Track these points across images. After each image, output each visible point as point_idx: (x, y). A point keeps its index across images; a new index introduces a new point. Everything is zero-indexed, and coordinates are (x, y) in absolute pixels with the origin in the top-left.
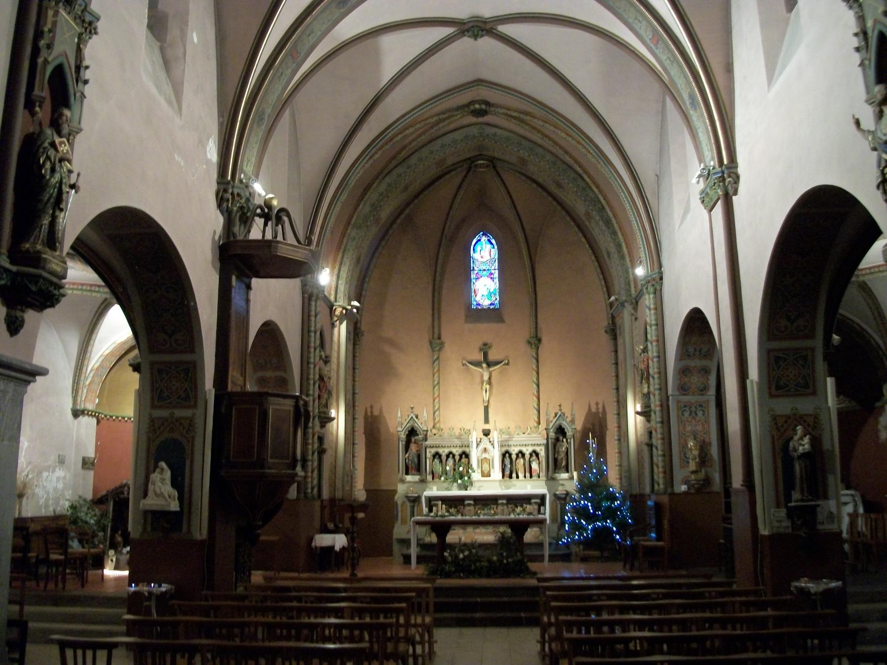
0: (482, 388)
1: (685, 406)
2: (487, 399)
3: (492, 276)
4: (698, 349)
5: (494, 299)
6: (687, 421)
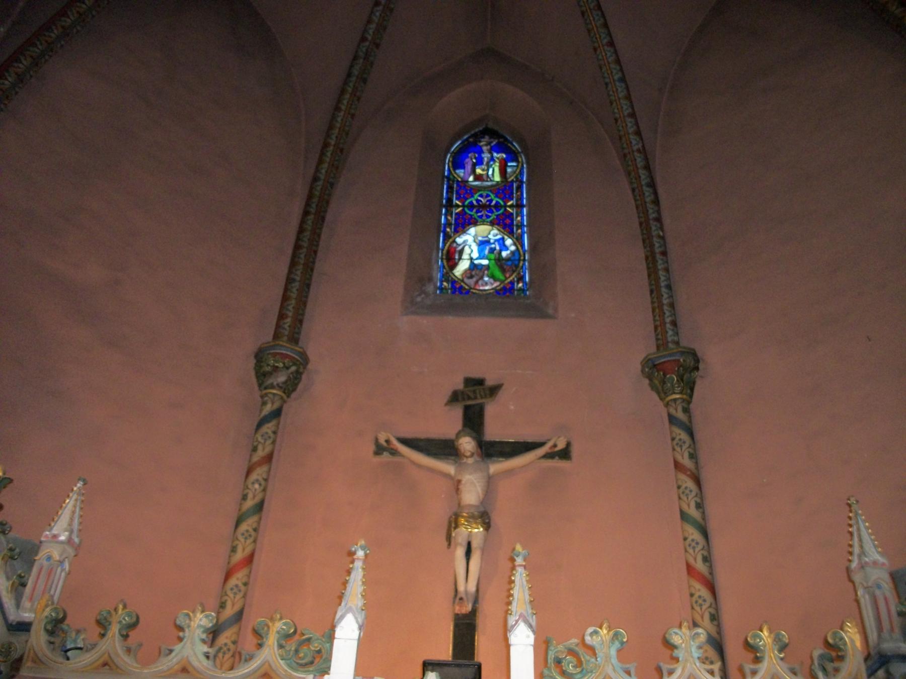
0: (449, 538)
2: (472, 587)
3: (508, 221)
5: (514, 277)
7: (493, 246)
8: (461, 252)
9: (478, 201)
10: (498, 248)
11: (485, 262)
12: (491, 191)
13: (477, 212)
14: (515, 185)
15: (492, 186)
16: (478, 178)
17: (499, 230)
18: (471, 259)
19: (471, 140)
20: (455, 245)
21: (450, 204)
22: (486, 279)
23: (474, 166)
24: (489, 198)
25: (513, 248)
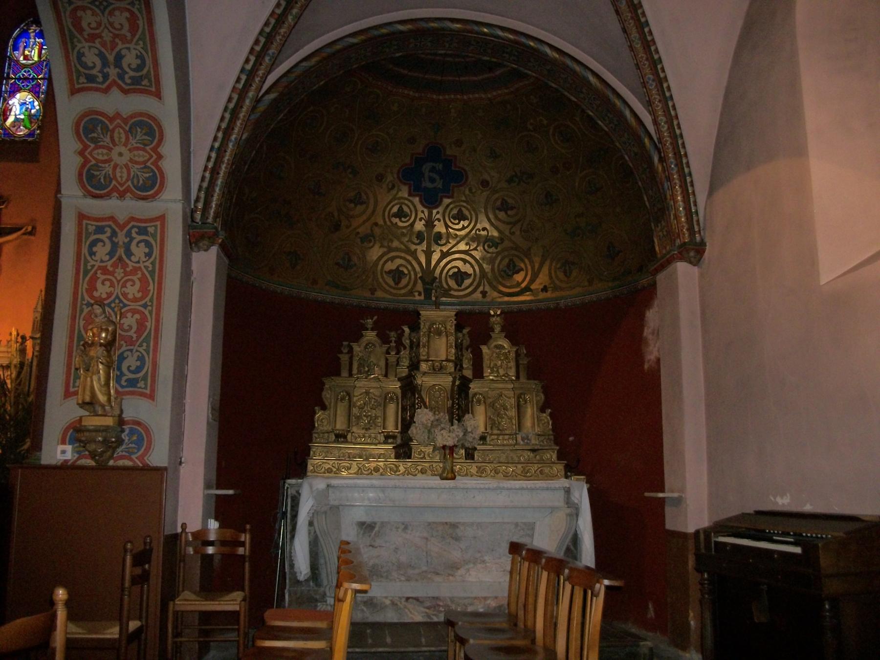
1: (100, 230)
4: (111, 58)
6: (105, 271)
7: (27, 106)
8: (11, 110)
9: (23, 75)
10: (30, 108)
11: (22, 117)
12: (30, 68)
13: (22, 83)
14: (45, 63)
15: (32, 64)
16: (26, 58)
17: (32, 95)
18: (16, 115)
19: (25, 28)
20: (8, 105)
21: (8, 78)
22: (22, 127)
23: (25, 47)
24: (29, 73)
25: (38, 108)
